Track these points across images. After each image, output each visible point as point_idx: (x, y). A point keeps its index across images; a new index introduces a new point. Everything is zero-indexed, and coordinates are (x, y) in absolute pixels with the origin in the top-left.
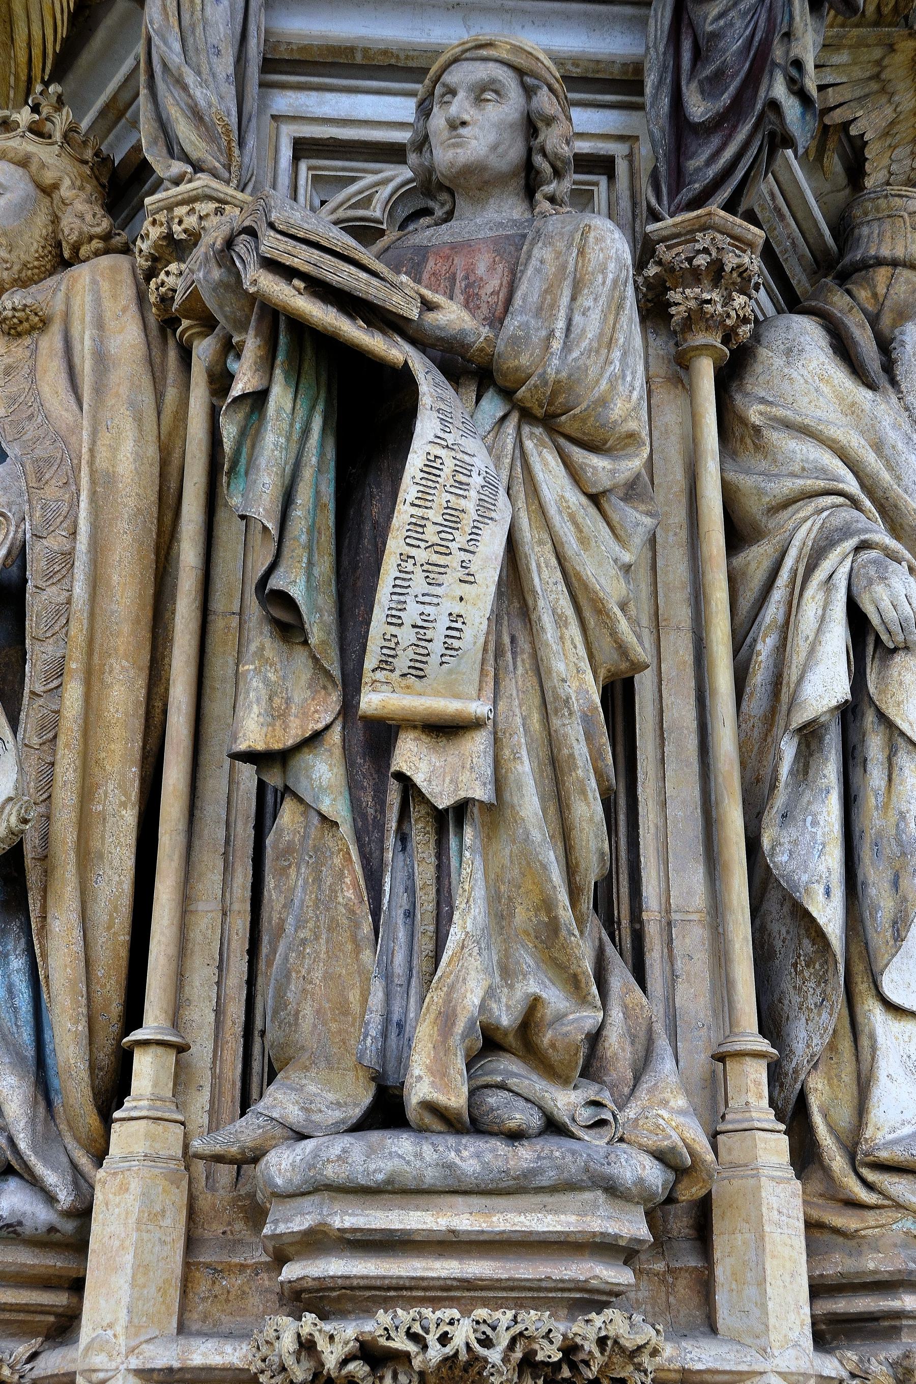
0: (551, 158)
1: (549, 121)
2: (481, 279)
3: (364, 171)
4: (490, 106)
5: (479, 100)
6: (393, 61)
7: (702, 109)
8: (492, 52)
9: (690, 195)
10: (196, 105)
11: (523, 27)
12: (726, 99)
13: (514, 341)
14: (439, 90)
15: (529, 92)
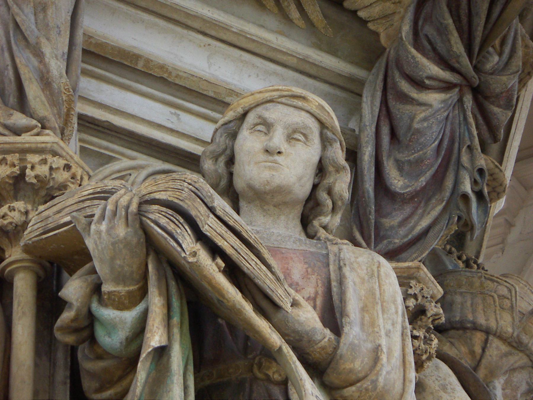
0: (336, 197)
1: (339, 169)
2: (297, 284)
3: (123, 154)
4: (299, 146)
5: (290, 138)
6: (165, 76)
7: (401, 183)
8: (305, 105)
9: (391, 247)
10: (48, 72)
11: (250, 76)
12: (423, 181)
13: (353, 347)
14: (251, 118)
15: (325, 142)
